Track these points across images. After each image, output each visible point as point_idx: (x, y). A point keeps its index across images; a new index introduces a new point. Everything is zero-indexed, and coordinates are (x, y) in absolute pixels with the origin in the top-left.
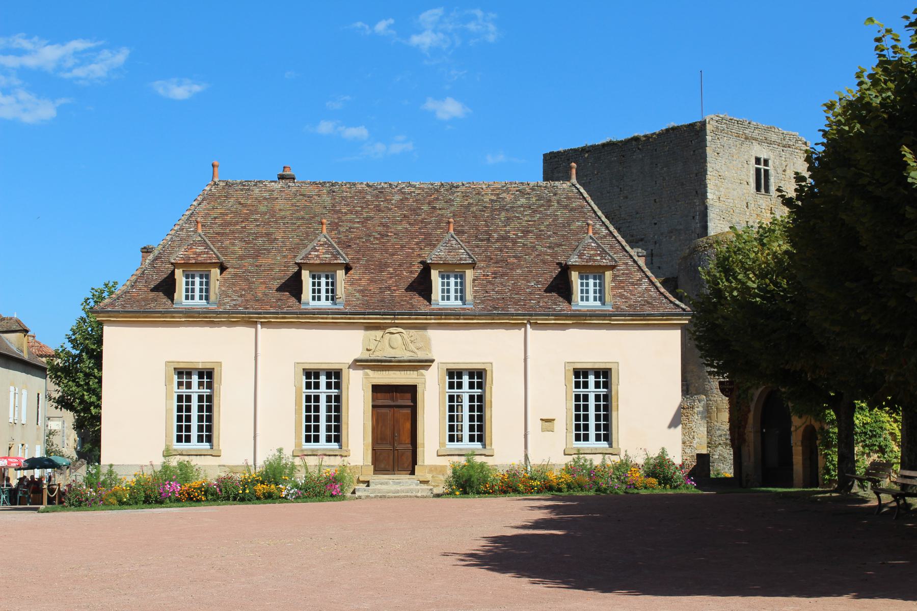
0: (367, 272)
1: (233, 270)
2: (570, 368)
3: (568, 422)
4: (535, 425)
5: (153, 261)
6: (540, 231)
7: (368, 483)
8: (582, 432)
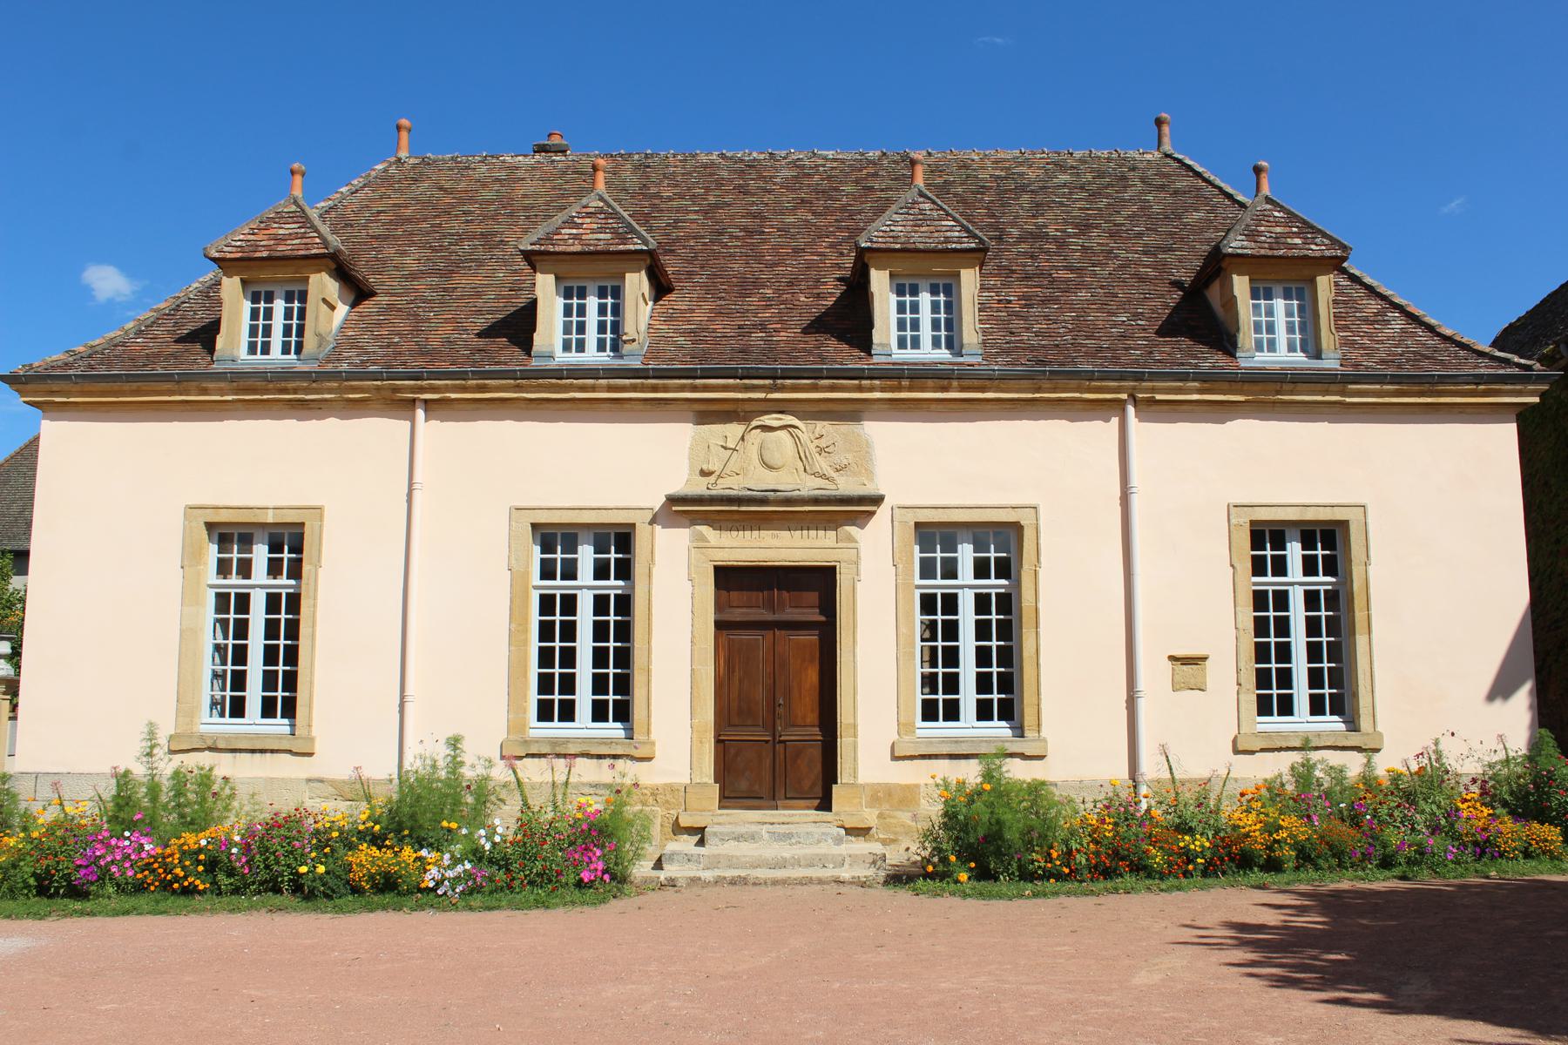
0: (710, 296)
1: (386, 298)
2: (1241, 521)
3: (1242, 665)
4: (1154, 674)
6: (1115, 225)
8: (1275, 692)
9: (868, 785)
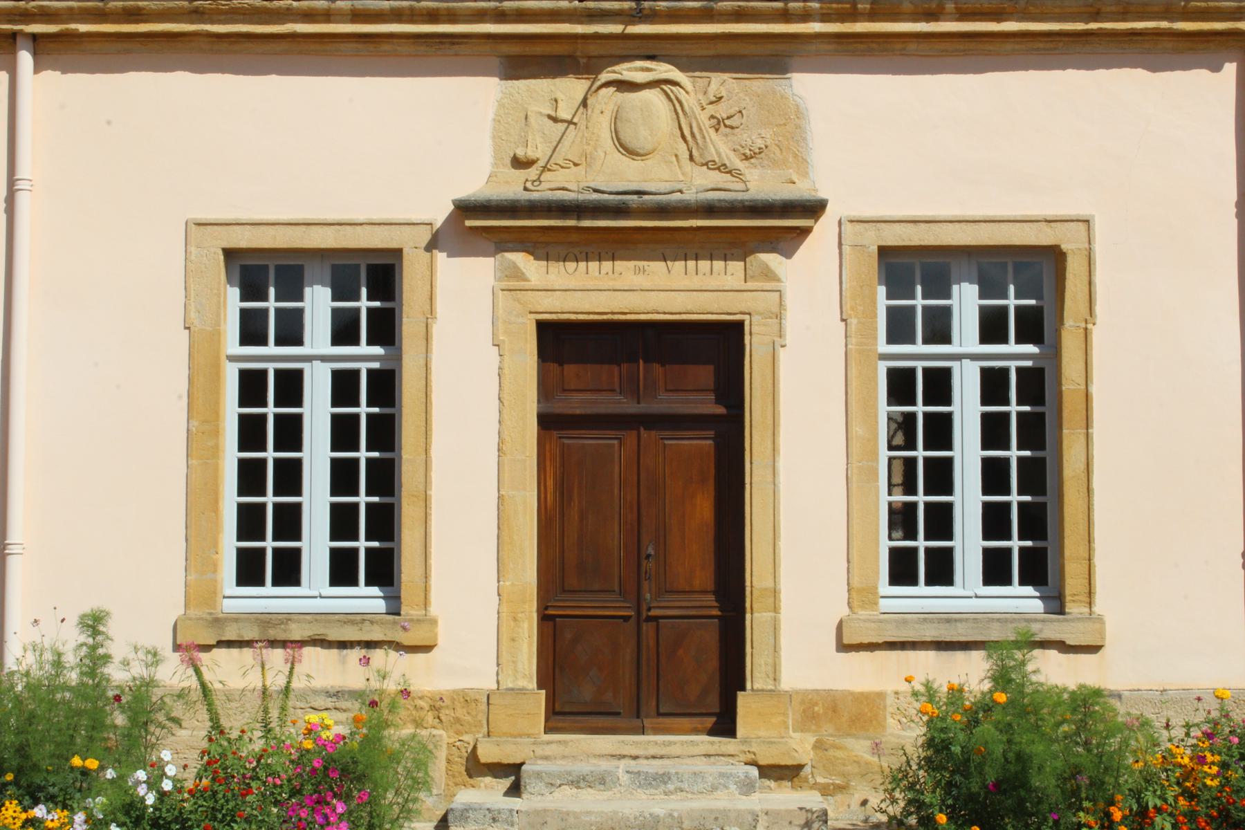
9: (797, 692)
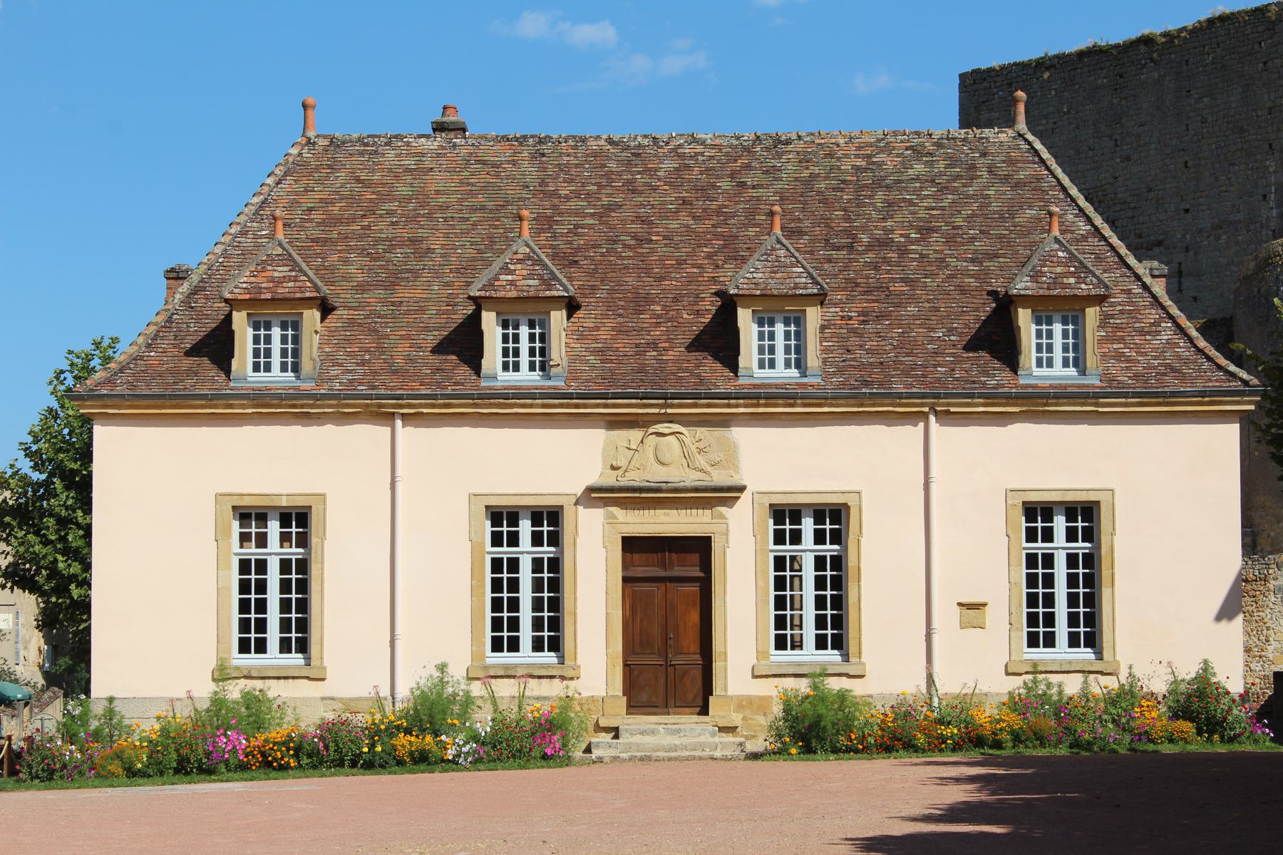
0: (611, 313)
1: (346, 312)
3: (1013, 610)
4: (946, 614)
5: (188, 297)
6: (954, 228)
7: (615, 731)
